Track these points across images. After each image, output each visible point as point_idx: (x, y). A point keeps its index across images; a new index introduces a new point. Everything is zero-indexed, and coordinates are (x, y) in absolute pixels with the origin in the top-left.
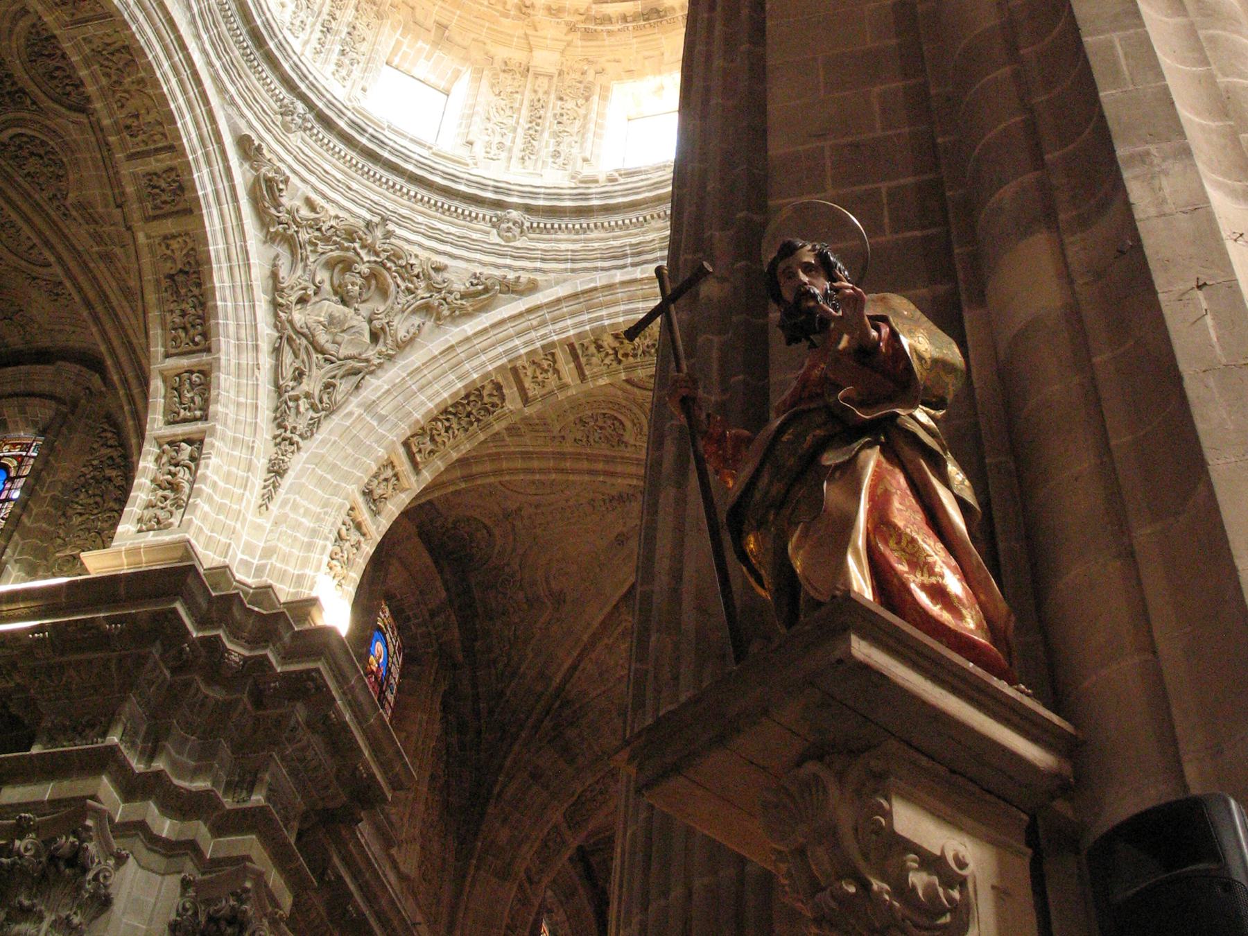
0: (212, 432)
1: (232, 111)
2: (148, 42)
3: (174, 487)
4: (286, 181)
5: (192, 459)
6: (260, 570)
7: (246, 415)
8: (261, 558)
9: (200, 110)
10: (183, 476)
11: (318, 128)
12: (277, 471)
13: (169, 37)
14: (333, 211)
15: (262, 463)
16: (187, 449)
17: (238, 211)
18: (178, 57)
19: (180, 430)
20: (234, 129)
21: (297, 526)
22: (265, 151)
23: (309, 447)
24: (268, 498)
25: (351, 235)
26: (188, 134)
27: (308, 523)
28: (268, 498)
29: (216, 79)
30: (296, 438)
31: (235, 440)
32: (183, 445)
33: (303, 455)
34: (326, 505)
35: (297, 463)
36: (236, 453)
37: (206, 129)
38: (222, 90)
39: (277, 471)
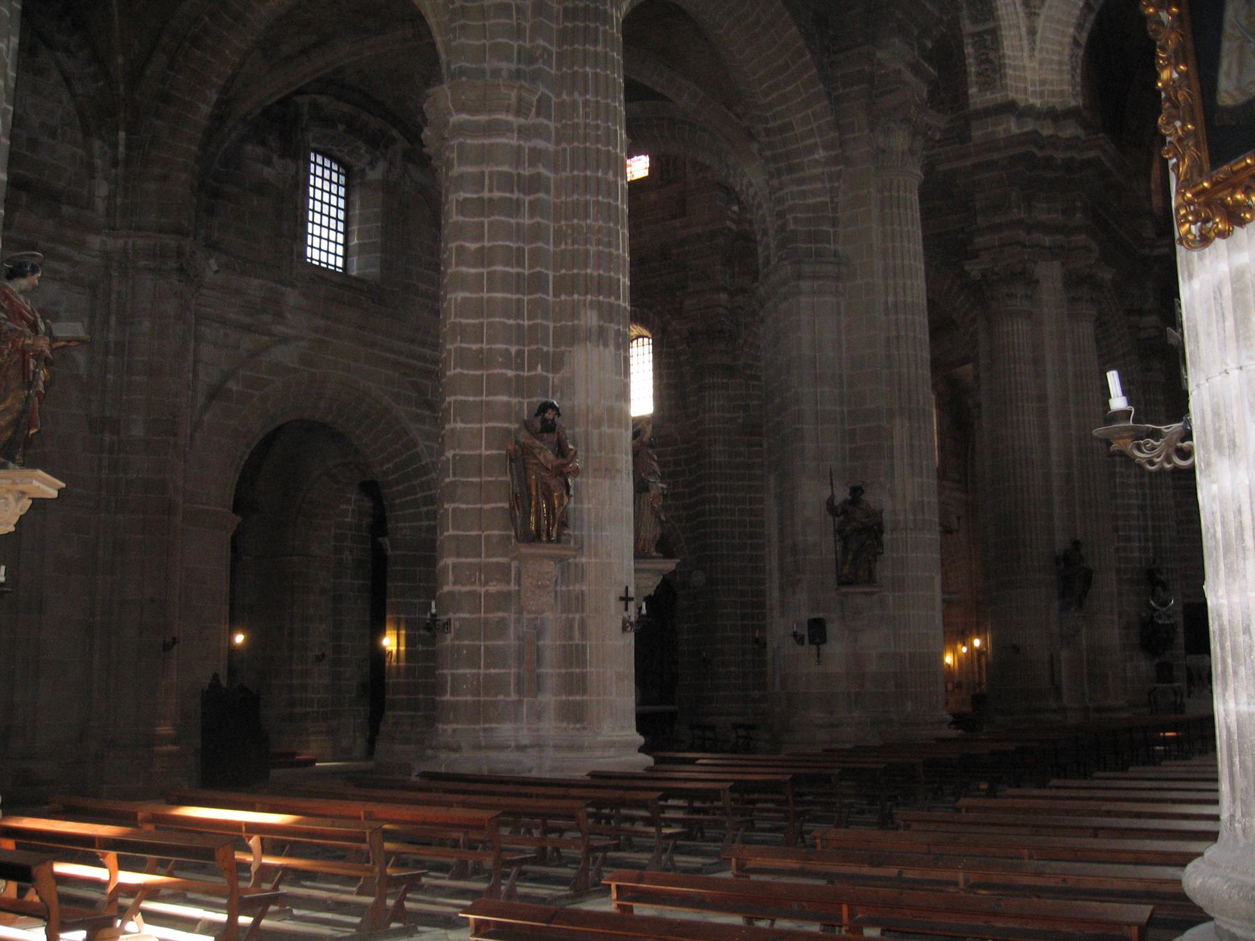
0: (999, 27)
3: (989, 61)
5: (993, 43)
6: (1042, 94)
7: (1011, 9)
8: (1040, 86)
10: (992, 55)
12: (1032, 32)
15: (1024, 30)
16: (988, 37)
19: (981, 28)
21: (1051, 61)
23: (1044, 12)
24: (1033, 49)
27: (1055, 58)
28: (1033, 49)
30: (1037, 11)
31: (1010, 25)
32: (986, 37)
33: (1042, 18)
34: (1061, 44)
35: (1041, 23)
36: (1012, 33)
39: (1032, 32)
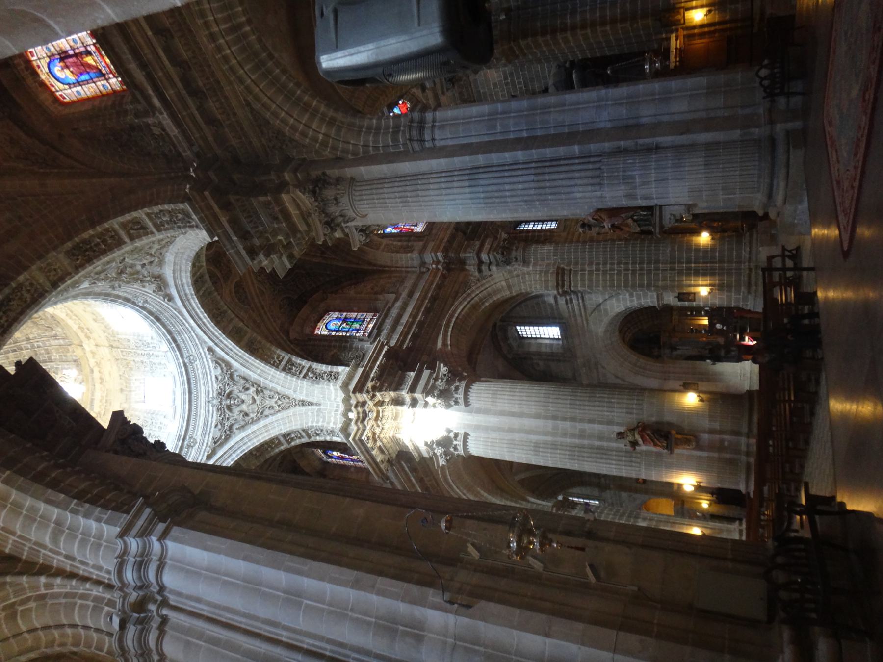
1: (175, 306)
2: (214, 328)
4: (154, 291)
9: (189, 308)
11: (129, 296)
13: (204, 328)
14: (135, 286)
17: (175, 282)
18: (200, 322)
20: (175, 302)
22: (162, 298)
25: (128, 283)
26: (195, 302)
29: (182, 315)
37: (187, 303)
38: (180, 312)
